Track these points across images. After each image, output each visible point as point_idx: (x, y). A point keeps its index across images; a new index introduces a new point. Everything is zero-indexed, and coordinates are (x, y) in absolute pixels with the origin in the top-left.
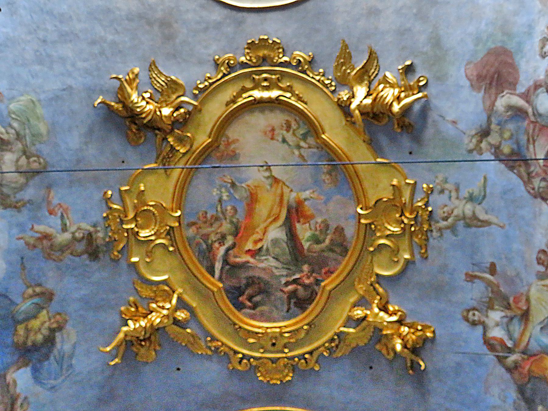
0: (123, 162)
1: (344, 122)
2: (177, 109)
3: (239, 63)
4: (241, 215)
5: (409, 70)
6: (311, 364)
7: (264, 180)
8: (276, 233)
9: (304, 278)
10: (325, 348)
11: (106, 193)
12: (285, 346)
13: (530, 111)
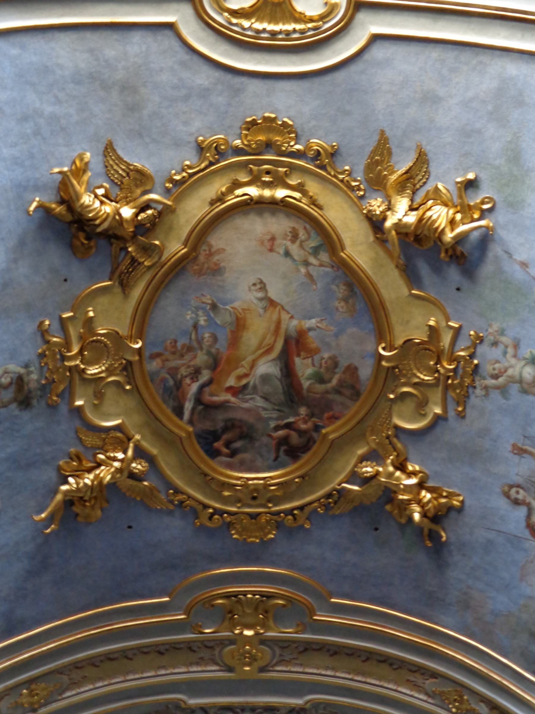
0: (66, 280)
1: (372, 238)
2: (143, 209)
3: (232, 147)
4: (222, 345)
6: (300, 522)
7: (255, 301)
8: (267, 367)
9: (300, 423)
10: (320, 503)
11: (42, 323)
12: (269, 501)
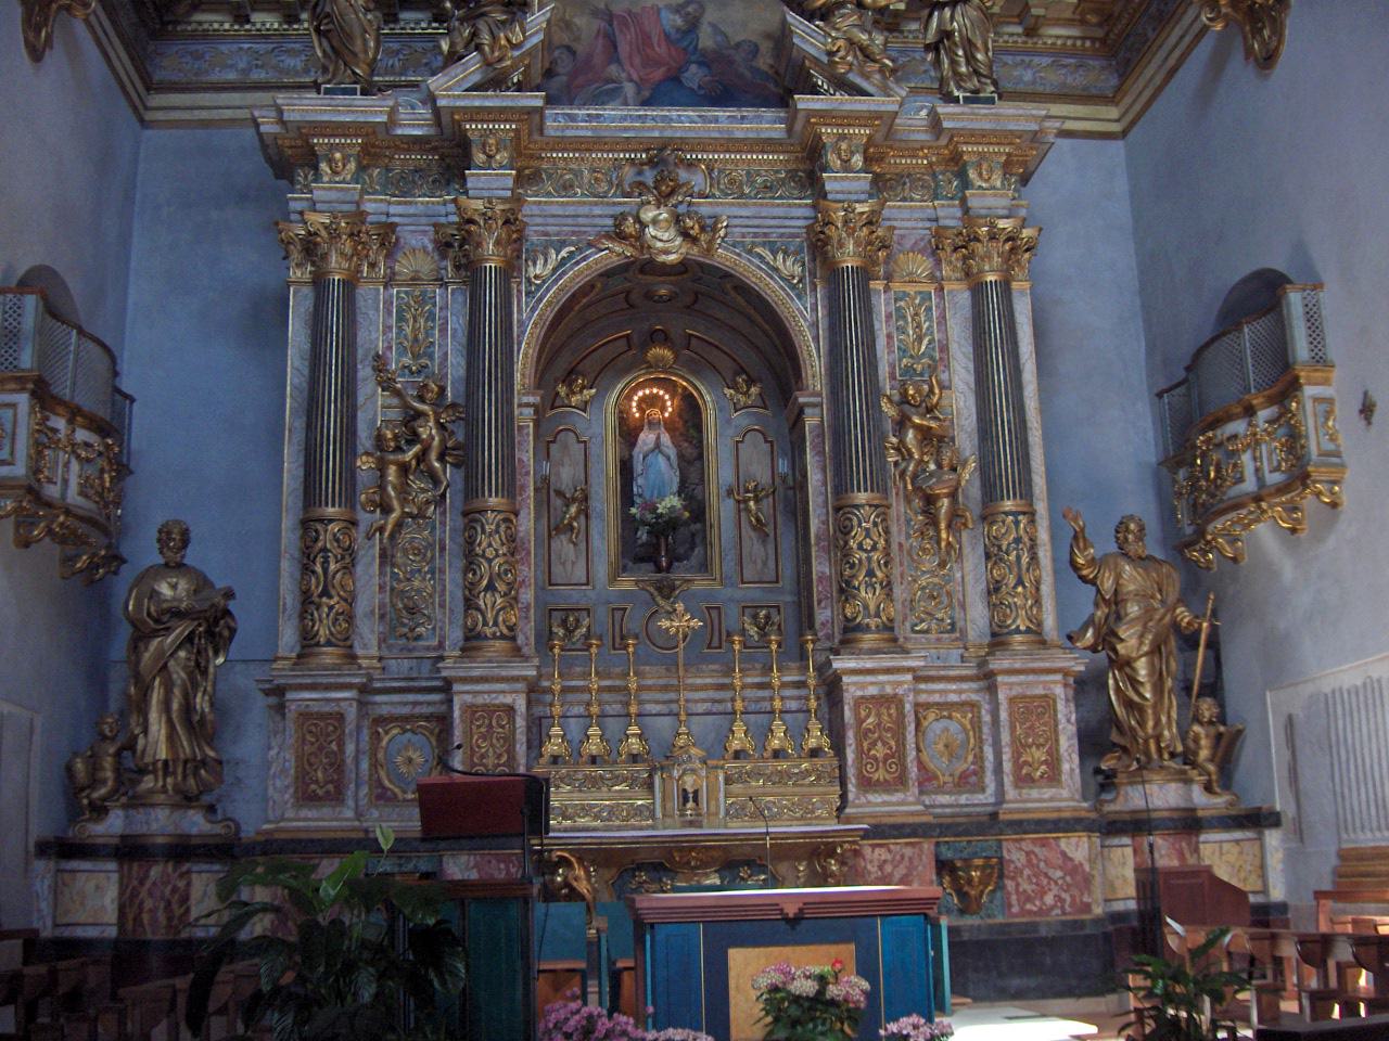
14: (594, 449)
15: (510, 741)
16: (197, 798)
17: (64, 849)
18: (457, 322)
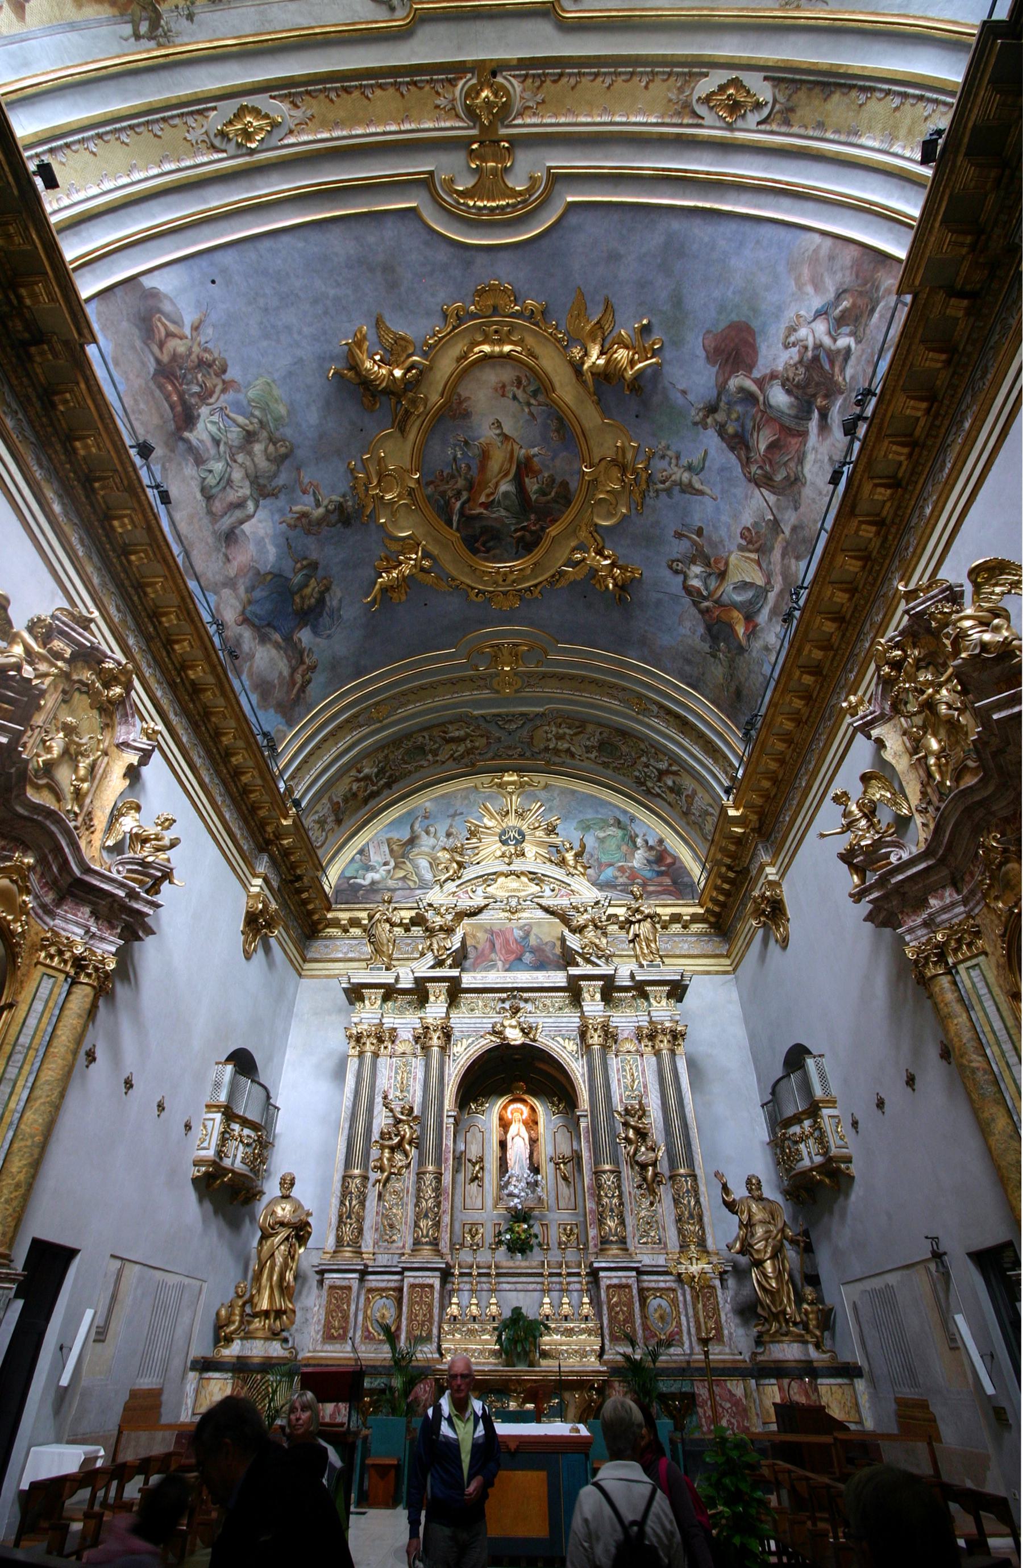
2: (408, 370)
4: (474, 472)
5: (646, 330)
8: (505, 487)
13: (761, 398)
14: (486, 1136)
15: (430, 1307)
16: (278, 1334)
17: (205, 1365)
18: (420, 1075)
